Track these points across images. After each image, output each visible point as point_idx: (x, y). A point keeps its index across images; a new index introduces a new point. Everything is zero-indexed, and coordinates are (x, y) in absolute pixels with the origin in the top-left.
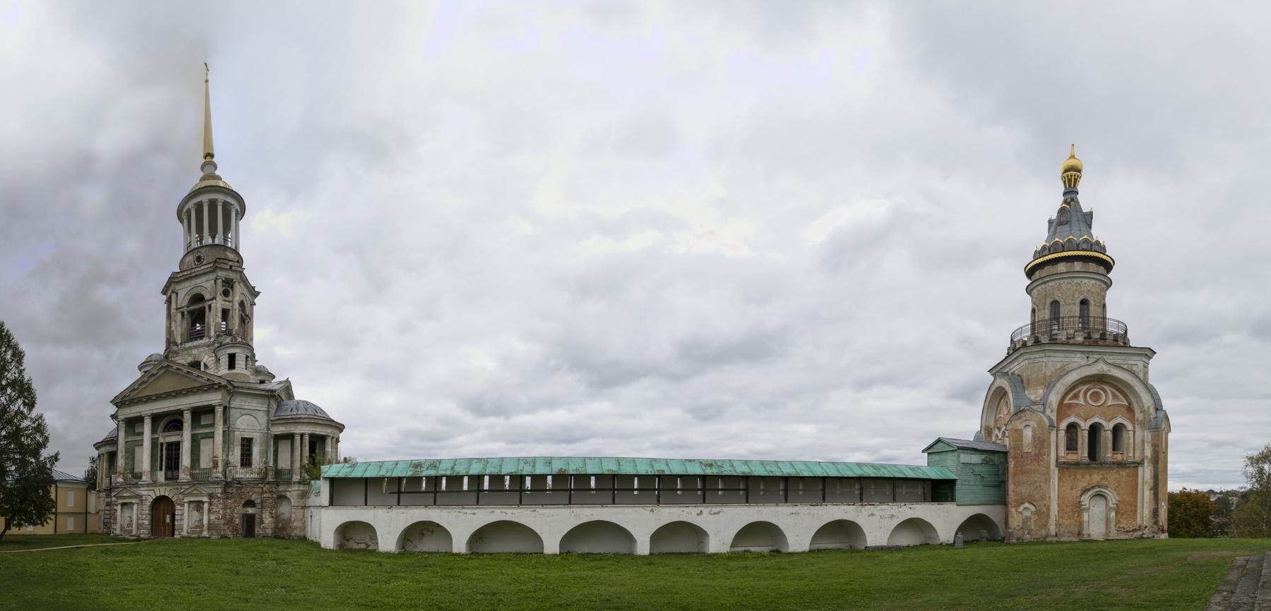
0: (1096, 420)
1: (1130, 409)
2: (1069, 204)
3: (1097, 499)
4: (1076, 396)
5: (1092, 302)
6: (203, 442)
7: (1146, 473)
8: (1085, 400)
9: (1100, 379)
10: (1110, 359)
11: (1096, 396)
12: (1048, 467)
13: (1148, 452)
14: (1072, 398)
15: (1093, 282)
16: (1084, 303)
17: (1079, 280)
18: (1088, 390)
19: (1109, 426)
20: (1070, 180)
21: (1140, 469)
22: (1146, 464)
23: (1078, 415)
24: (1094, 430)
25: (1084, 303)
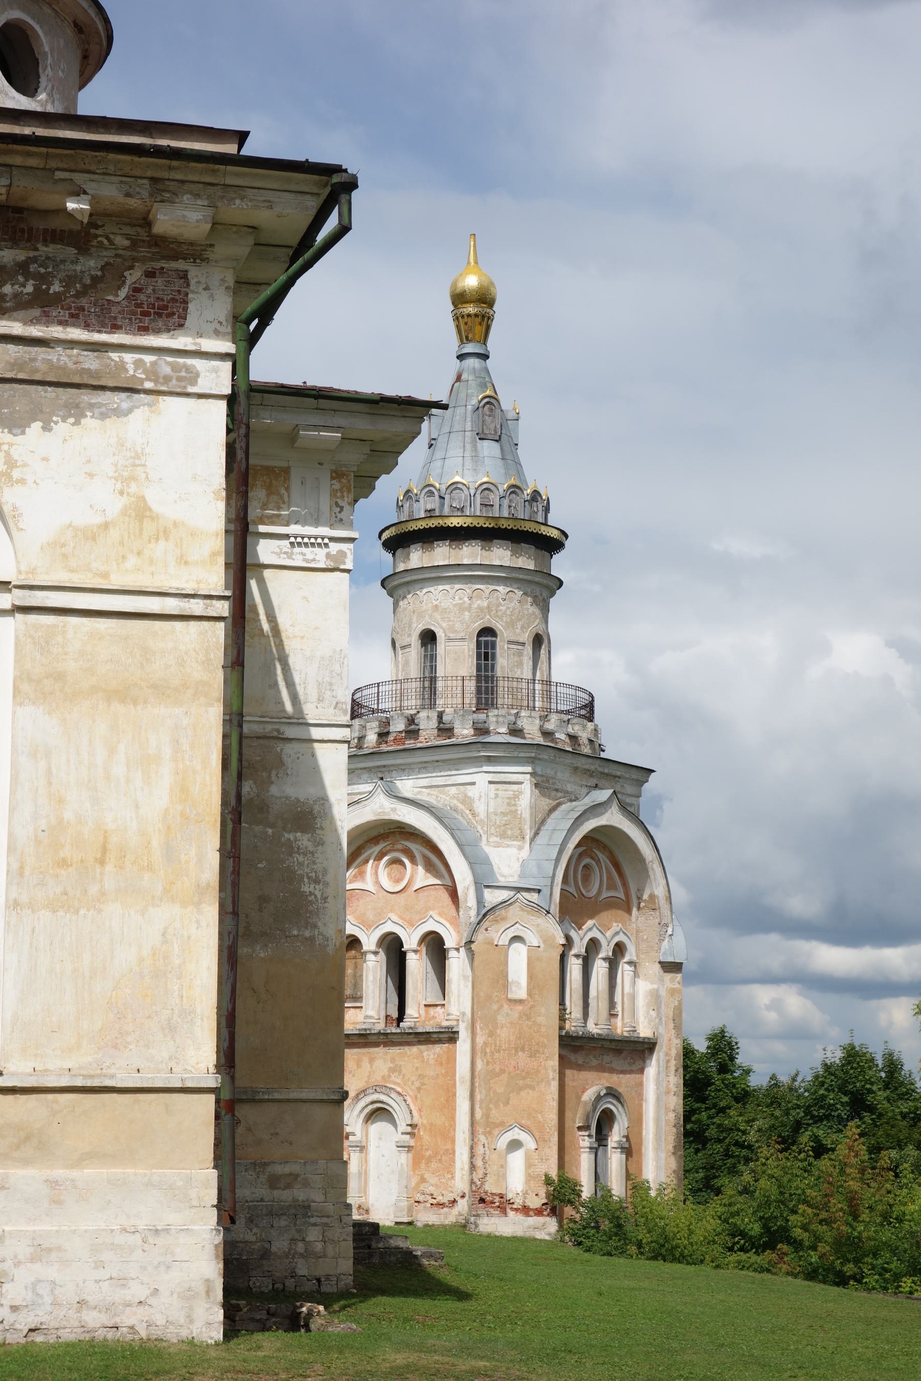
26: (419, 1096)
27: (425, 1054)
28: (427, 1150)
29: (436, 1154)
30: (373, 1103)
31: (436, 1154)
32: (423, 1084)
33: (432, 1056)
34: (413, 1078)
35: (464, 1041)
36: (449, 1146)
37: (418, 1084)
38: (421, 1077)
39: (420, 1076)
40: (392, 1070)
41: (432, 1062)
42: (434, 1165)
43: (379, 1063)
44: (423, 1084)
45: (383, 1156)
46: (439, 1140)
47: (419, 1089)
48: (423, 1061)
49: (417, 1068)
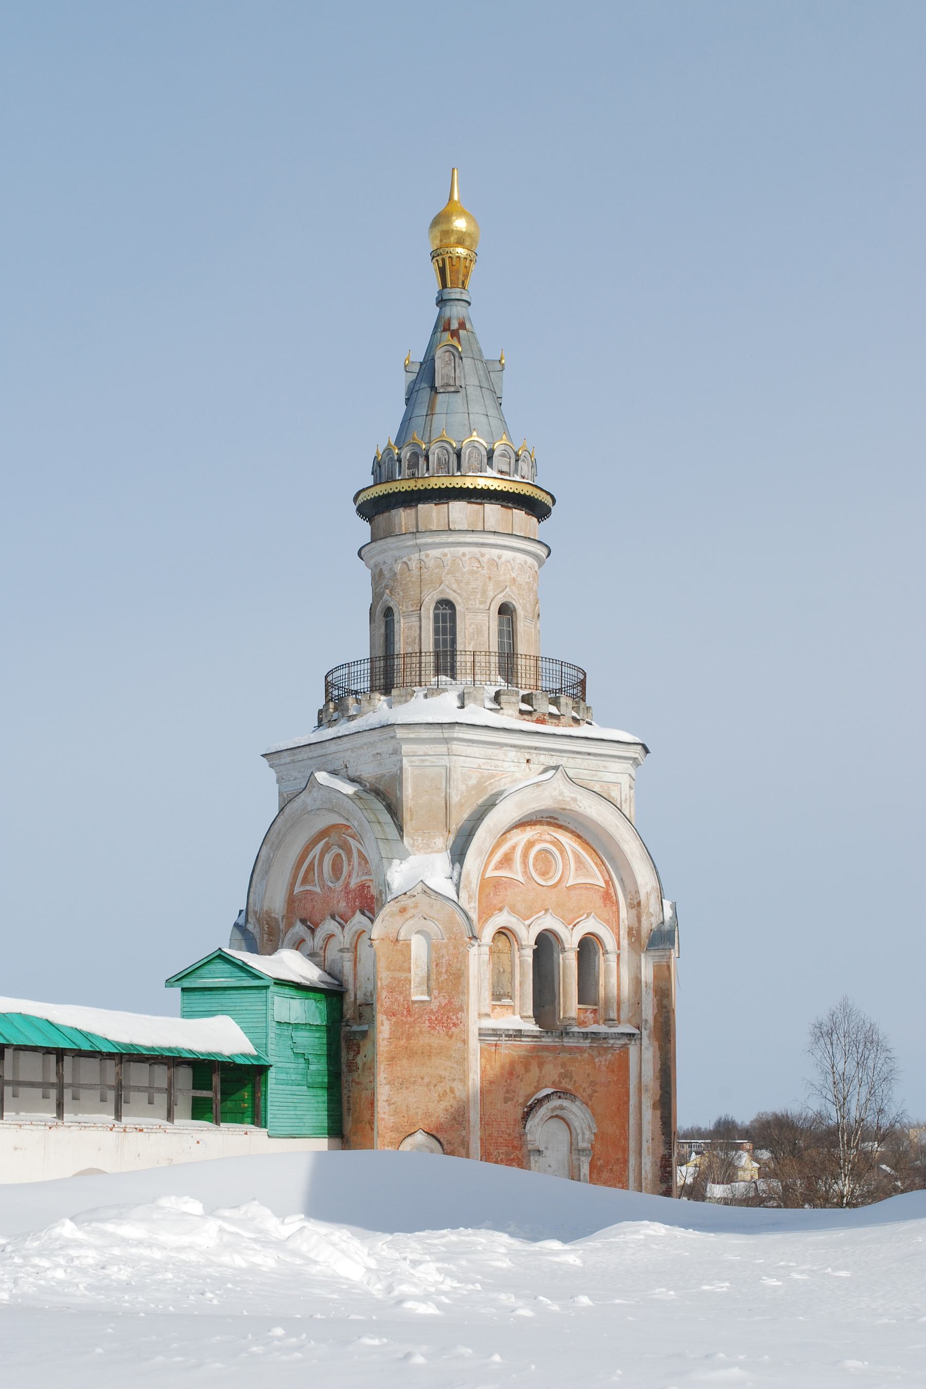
0: (549, 922)
1: (608, 898)
2: (455, 334)
3: (555, 1125)
4: (507, 860)
5: (520, 612)
6: (6, 1050)
7: (643, 1061)
8: (525, 872)
9: (550, 819)
10: (575, 766)
11: (545, 861)
12: (465, 1042)
13: (649, 1011)
14: (496, 868)
15: (521, 557)
16: (505, 610)
17: (495, 552)
18: (530, 844)
19: (571, 939)
20: (455, 272)
21: (633, 1050)
22: (645, 1033)
23: (513, 910)
24: (546, 944)
25: (505, 610)
26: (590, 1103)
27: (597, 1060)
28: (599, 1159)
29: (608, 1163)
30: (553, 1110)
31: (608, 1163)
32: (595, 1091)
33: (603, 1063)
34: (585, 1085)
35: (647, 1048)
36: (620, 1155)
37: (589, 1091)
38: (593, 1084)
39: (592, 1082)
40: (562, 1076)
41: (604, 1069)
42: (605, 1175)
43: (548, 1067)
44: (595, 1091)
45: (550, 1166)
46: (610, 1148)
47: (590, 1096)
48: (595, 1068)
49: (589, 1075)
